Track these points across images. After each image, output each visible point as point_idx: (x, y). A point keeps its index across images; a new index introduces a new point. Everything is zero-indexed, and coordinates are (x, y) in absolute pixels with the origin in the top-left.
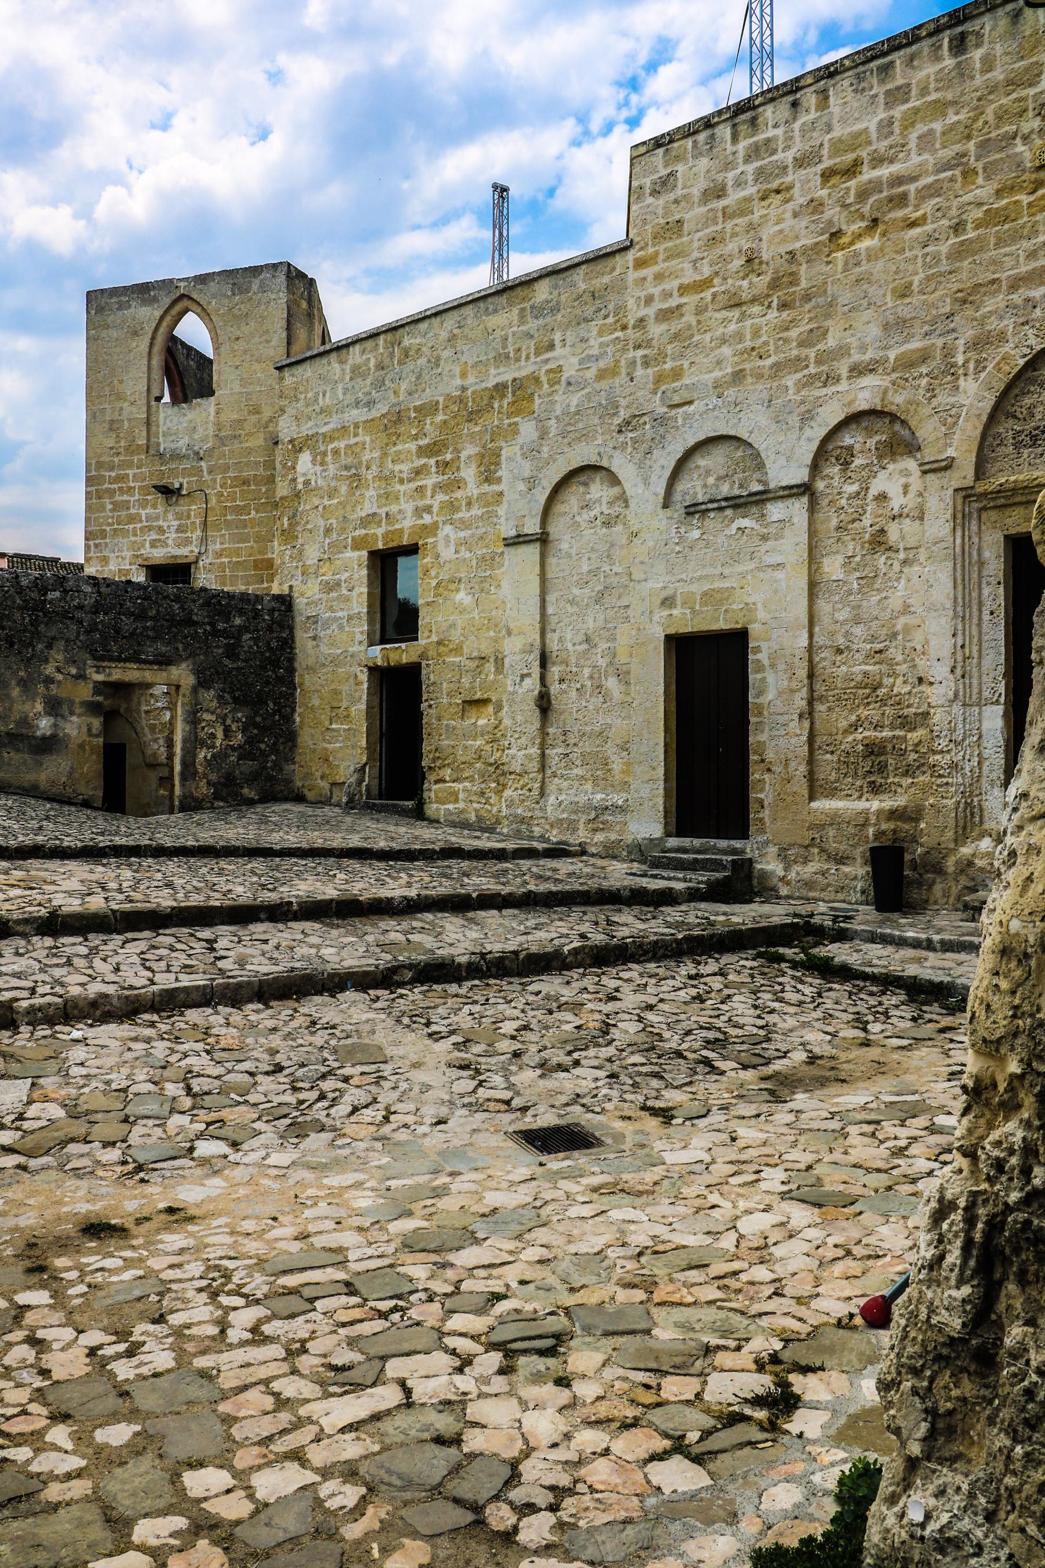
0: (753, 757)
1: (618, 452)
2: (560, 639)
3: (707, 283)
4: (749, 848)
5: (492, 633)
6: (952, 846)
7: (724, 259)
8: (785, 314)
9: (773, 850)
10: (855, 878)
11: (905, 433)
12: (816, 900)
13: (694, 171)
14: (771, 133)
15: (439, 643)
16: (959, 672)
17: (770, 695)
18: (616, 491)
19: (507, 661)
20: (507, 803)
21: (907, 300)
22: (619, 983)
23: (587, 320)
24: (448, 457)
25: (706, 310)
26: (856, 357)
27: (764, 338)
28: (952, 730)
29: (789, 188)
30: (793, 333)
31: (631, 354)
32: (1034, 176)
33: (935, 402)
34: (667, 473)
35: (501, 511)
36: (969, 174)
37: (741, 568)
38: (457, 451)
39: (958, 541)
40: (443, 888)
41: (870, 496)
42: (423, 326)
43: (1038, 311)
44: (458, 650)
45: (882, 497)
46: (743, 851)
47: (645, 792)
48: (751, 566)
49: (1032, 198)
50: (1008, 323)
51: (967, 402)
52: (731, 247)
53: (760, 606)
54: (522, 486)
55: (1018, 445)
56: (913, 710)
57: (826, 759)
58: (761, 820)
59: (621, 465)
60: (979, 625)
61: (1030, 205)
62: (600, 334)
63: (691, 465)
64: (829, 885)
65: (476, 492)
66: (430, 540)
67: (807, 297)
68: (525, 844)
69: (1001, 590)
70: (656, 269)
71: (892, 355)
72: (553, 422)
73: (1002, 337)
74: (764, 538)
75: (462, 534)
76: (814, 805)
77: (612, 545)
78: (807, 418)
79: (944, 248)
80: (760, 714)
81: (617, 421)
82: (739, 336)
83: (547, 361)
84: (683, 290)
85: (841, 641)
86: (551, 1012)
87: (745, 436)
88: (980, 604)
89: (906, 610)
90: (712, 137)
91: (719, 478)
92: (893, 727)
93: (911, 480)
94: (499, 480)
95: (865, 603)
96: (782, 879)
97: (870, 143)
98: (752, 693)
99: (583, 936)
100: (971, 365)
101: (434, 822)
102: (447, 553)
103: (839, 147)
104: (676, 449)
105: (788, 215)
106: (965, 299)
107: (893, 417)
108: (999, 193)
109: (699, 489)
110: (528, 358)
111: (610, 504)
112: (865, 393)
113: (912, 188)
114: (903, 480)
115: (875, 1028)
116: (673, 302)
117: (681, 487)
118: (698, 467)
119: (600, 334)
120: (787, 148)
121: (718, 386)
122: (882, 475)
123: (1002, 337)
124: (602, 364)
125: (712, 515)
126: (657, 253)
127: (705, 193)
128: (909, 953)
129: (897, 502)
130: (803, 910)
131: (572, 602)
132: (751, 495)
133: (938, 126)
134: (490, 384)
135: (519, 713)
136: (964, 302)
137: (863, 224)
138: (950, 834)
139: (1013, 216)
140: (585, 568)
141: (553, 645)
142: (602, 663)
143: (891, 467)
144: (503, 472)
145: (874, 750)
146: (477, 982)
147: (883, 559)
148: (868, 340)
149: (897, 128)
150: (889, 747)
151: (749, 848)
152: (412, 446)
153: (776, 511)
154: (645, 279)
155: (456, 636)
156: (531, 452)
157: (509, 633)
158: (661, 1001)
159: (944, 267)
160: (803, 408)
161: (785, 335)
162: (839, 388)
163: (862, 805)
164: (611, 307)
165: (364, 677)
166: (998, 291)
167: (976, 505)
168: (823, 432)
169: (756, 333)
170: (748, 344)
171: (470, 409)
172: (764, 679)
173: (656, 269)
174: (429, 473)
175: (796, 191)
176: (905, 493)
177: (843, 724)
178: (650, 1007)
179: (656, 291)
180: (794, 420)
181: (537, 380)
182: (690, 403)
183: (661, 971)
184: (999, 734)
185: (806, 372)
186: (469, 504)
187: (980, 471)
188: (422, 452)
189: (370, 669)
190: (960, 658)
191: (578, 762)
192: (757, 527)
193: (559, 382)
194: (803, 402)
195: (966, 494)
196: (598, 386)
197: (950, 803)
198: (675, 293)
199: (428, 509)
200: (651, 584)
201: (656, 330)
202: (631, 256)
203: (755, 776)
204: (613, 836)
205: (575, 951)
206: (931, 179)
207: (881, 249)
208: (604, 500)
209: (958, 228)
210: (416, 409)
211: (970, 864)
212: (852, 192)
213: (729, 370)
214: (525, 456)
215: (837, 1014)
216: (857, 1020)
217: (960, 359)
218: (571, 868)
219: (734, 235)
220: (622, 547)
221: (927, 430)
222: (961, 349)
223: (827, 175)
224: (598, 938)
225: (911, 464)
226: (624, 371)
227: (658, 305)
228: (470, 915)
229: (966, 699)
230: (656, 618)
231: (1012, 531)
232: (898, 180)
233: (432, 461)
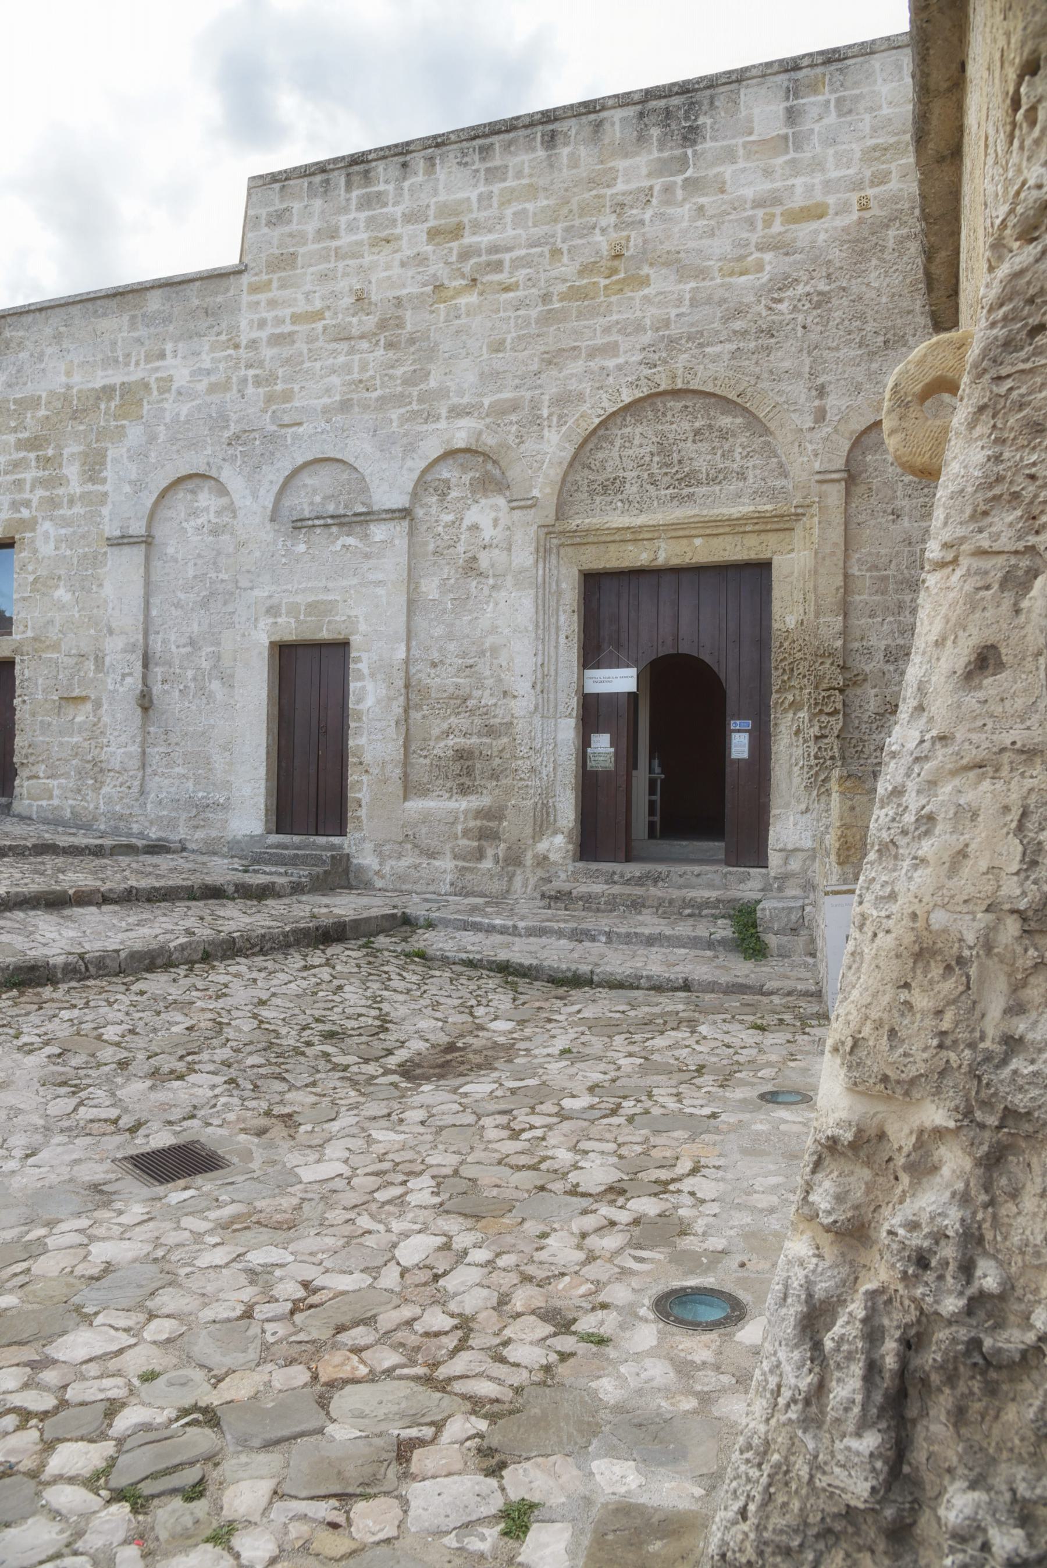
0: (352, 760)
1: (226, 465)
2: (163, 642)
3: (318, 315)
4: (345, 843)
5: (92, 632)
6: (531, 842)
7: (334, 295)
8: (390, 354)
9: (369, 846)
10: (445, 871)
11: (497, 472)
12: (410, 893)
13: (308, 214)
14: (381, 187)
15: (35, 639)
16: (538, 687)
17: (369, 702)
18: (224, 501)
19: (108, 659)
20: (106, 800)
21: (500, 355)
22: (229, 978)
23: (200, 335)
24: (50, 452)
25: (317, 339)
26: (455, 400)
27: (371, 373)
28: (532, 739)
29: (398, 238)
30: (399, 372)
31: (243, 372)
32: (609, 264)
33: (523, 447)
34: (276, 488)
35: (105, 511)
36: (556, 253)
37: (345, 583)
38: (59, 447)
39: (540, 572)
40: (35, 885)
41: (464, 526)
42: (29, 318)
43: (611, 378)
44: (55, 647)
45: (475, 528)
46: (341, 847)
47: (247, 791)
48: (355, 581)
49: (607, 281)
50: (586, 387)
51: (550, 450)
52: (342, 285)
53: (361, 619)
54: (127, 489)
55: (592, 493)
56: (498, 720)
57: (421, 763)
58: (358, 818)
59: (229, 476)
60: (556, 647)
61: (606, 287)
62: (212, 349)
63: (297, 482)
64: (421, 878)
65: (78, 490)
66: (28, 535)
67: (412, 341)
68: (124, 841)
69: (575, 617)
70: (270, 295)
71: (486, 402)
72: (162, 428)
73: (581, 397)
74: (367, 556)
75: (63, 531)
76: (409, 804)
77: (219, 553)
78: (410, 449)
79: (534, 313)
80: (360, 719)
81: (227, 434)
82: (347, 368)
83: (157, 369)
84: (296, 318)
85: (435, 656)
86: (158, 1013)
87: (351, 460)
88: (558, 629)
89: (494, 630)
90: (327, 181)
91: (325, 498)
92: (480, 735)
93: (501, 515)
94: (104, 481)
95: (457, 622)
96: (377, 873)
97: (471, 211)
98: (352, 698)
99: (189, 932)
100: (555, 419)
101: (23, 818)
102: (47, 549)
103: (443, 210)
104: (286, 466)
105: (397, 263)
106: (551, 360)
107: (486, 456)
108: (581, 273)
109: (305, 506)
110: (137, 364)
111: (218, 513)
112: (461, 433)
113: (507, 257)
114: (493, 515)
115: (480, 1011)
116: (287, 328)
117: (287, 503)
118: (305, 485)
119: (212, 349)
120: (396, 203)
121: (326, 410)
122: (475, 508)
123: (581, 397)
124: (213, 379)
125: (318, 531)
126: (270, 281)
127: (319, 231)
128: (498, 938)
129: (488, 533)
130: (396, 901)
131: (177, 605)
132: (356, 515)
133: (530, 206)
134: (98, 384)
135: (118, 715)
136: (550, 363)
137: (464, 282)
138: (529, 831)
139: (592, 295)
140: (191, 573)
141: (157, 645)
142: (205, 665)
143: (483, 501)
144: (108, 473)
145: (462, 755)
146: (73, 984)
147: (474, 583)
148: (466, 385)
149: (495, 201)
150: (477, 753)
151: (345, 843)
152: (11, 438)
153: (379, 532)
154: (258, 303)
155: (53, 634)
156: (139, 455)
157: (111, 632)
158: (274, 995)
159: (533, 329)
160: (405, 441)
161: (391, 371)
162: (439, 426)
163: (452, 805)
164: (224, 325)
166: (578, 357)
167: (555, 541)
168: (423, 465)
169: (363, 368)
170: (356, 376)
171: (77, 408)
172: (363, 688)
173: (270, 295)
174: (28, 467)
175: (404, 243)
176: (495, 526)
177: (436, 732)
178: (262, 1003)
179: (269, 316)
180: (397, 450)
181: (147, 386)
182: (300, 424)
183: (270, 965)
184: (571, 743)
185: (409, 408)
186: (71, 502)
187: (561, 511)
188: (21, 445)
190: (539, 676)
191: (180, 761)
192: (360, 545)
193: (169, 390)
194: (405, 435)
195: (548, 530)
196: (208, 399)
197: (529, 803)
198: (288, 321)
199: (27, 504)
200: (256, 592)
201: (268, 353)
202: (245, 279)
203: (353, 777)
204: (214, 834)
205: (182, 948)
206: (523, 252)
207: (480, 306)
208: (212, 509)
209: (546, 298)
210: (15, 401)
211: (546, 858)
212: (455, 252)
213: (338, 398)
214: (131, 459)
215: (442, 1000)
216: (462, 1005)
217: (545, 413)
218: (172, 864)
219: (346, 275)
220: (228, 556)
221: (515, 473)
222: (546, 404)
223: (433, 234)
224: (204, 933)
225: (501, 501)
226: (235, 388)
227: (269, 330)
228: (67, 912)
229: (544, 709)
230: (261, 625)
231: (587, 567)
232: (494, 249)
233: (32, 455)
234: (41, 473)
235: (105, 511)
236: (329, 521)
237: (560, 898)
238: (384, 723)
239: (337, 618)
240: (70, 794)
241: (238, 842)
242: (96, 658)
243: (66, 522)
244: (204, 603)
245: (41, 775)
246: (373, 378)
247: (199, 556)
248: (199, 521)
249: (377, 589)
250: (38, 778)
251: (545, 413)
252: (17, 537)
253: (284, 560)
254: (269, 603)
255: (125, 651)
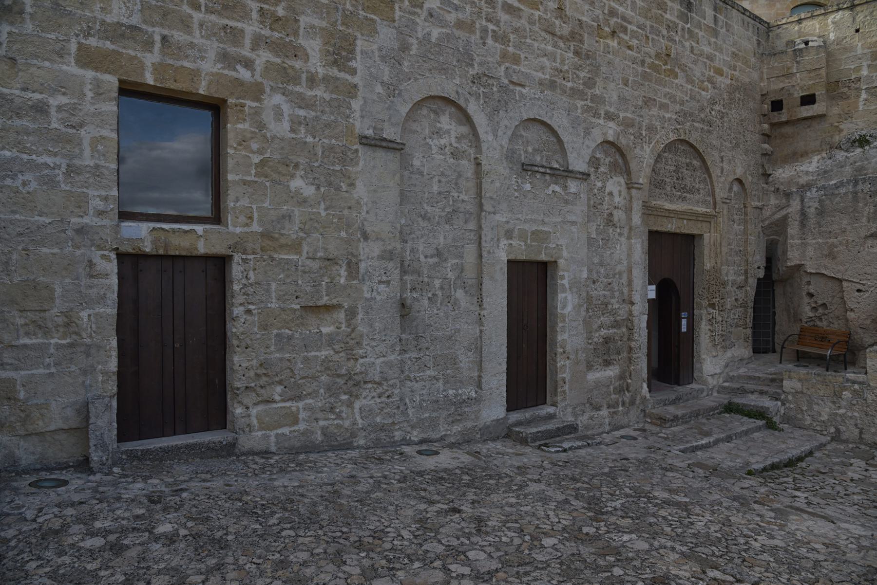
2: (413, 250)
5: (343, 234)
15: (265, 235)
17: (569, 308)
19: (362, 265)
27: (566, 67)
35: (356, 105)
44: (296, 247)
53: (564, 248)
58: (564, 392)
65: (321, 71)
74: (566, 202)
75: (302, 113)
77: (460, 176)
81: (471, 72)
131: (424, 217)
140: (435, 188)
142: (451, 275)
143: (615, 178)
157: (366, 237)
165: (112, 267)
172: (566, 297)
189: (122, 257)
200: (498, 217)
204: (469, 424)
214: (383, 58)
222: (644, 128)
230: (502, 245)
234: (266, 32)
235: (356, 105)
236: (548, 171)
237: (662, 421)
238: (576, 323)
239: (550, 245)
240: (320, 415)
241: (488, 427)
242: (349, 264)
243: (302, 102)
244: (449, 220)
245: (277, 398)
246: (567, 71)
247: (443, 174)
248: (443, 142)
249: (572, 228)
250: (275, 402)
251: (644, 133)
252: (231, 101)
253: (516, 194)
254: (507, 227)
255: (381, 258)
